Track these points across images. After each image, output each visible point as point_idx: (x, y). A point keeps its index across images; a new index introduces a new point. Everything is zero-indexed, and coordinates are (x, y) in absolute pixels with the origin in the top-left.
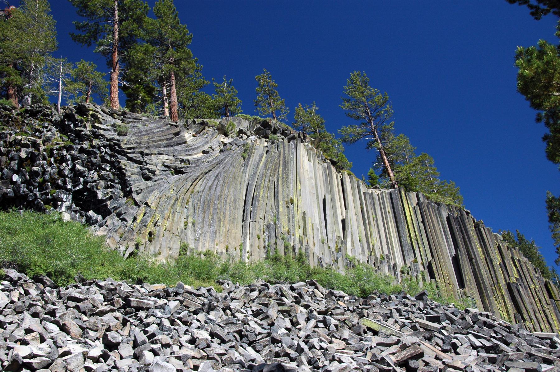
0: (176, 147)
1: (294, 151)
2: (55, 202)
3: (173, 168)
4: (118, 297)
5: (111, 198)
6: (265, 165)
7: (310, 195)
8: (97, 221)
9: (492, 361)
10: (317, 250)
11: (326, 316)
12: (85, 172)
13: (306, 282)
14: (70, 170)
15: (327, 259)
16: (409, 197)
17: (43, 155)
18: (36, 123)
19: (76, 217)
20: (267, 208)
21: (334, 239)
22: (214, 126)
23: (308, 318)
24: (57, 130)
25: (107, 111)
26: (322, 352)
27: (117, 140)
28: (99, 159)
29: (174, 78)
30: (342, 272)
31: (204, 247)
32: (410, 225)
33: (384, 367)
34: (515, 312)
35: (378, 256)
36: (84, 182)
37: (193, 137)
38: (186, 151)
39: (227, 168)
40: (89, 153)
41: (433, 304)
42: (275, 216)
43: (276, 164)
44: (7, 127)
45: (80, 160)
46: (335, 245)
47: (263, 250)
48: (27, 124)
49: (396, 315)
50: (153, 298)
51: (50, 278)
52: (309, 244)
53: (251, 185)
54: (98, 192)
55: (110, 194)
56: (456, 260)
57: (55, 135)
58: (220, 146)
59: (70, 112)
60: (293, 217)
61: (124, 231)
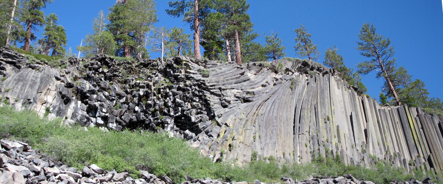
0: (243, 83)
1: (328, 82)
2: (163, 125)
3: (242, 99)
5: (201, 121)
6: (307, 93)
8: (192, 137)
10: (348, 153)
13: (344, 176)
14: (172, 102)
15: (357, 159)
16: (411, 111)
17: (154, 92)
18: (147, 71)
19: (177, 134)
20: (311, 124)
22: (268, 67)
24: (162, 75)
25: (194, 60)
27: (203, 81)
28: (191, 94)
29: (237, 34)
30: (368, 167)
32: (413, 131)
36: (181, 110)
39: (280, 97)
40: (184, 90)
42: (317, 130)
43: (315, 92)
44: (130, 75)
45: (179, 95)
46: (361, 148)
48: (142, 72)
51: (169, 177)
54: (192, 117)
55: (200, 118)
57: (161, 79)
58: (273, 81)
59: (170, 62)
60: (330, 130)
61: (212, 144)
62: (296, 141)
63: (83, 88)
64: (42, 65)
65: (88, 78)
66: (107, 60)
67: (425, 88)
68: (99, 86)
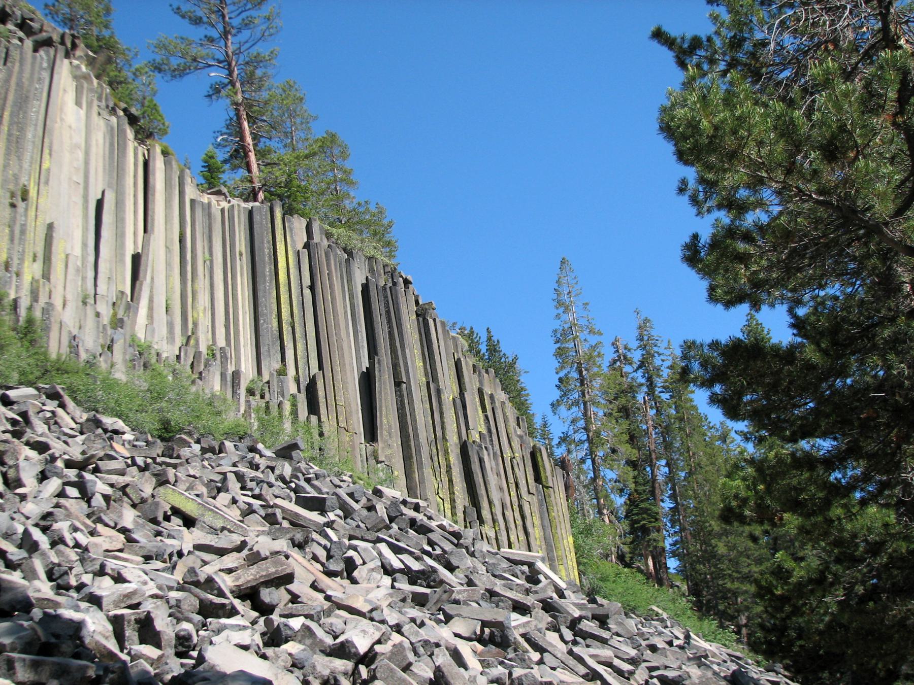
1: (46, 75)
9: (420, 601)
11: (84, 473)
13: (38, 389)
15: (90, 342)
21: (110, 297)
23: (42, 472)
26: (76, 552)
30: (120, 375)
33: (211, 597)
34: (467, 504)
35: (203, 349)
41: (311, 471)
46: (112, 311)
49: (234, 485)
52: (52, 301)
56: (368, 381)
60: (23, 232)
67: (348, 165)
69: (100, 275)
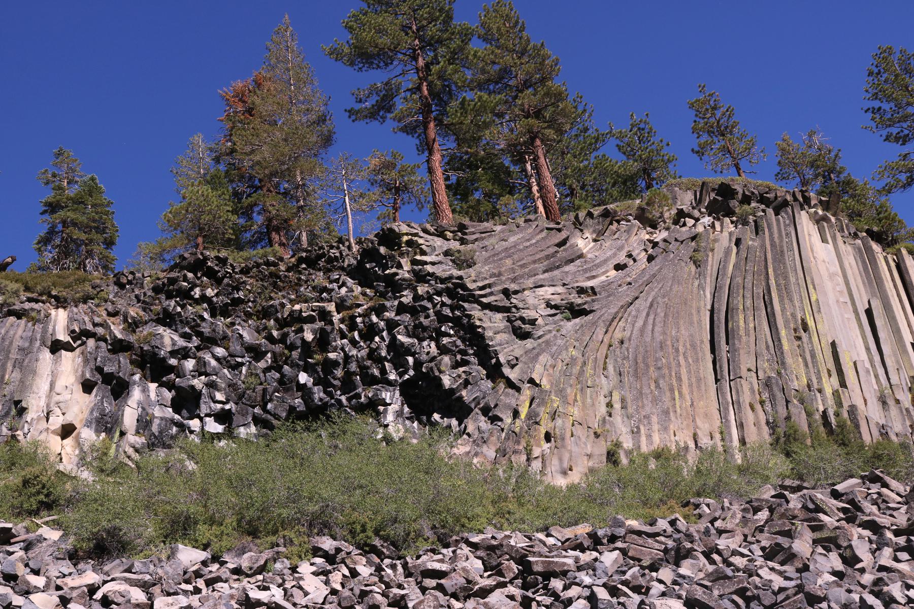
0: (567, 268)
2: (374, 407)
3: (566, 308)
4: (508, 560)
5: (466, 383)
7: (839, 307)
12: (413, 346)
17: (341, 330)
18: (319, 278)
19: (414, 428)
21: (904, 384)
28: (433, 317)
31: (652, 443)
37: (592, 244)
38: (585, 271)
40: (413, 310)
47: (766, 430)
48: (306, 282)
50: (571, 553)
53: (719, 311)
54: (442, 377)
55: (464, 376)
58: (646, 250)
59: (370, 245)
60: (813, 356)
62: (725, 398)
63: (157, 347)
64: (43, 302)
65: (167, 319)
66: (209, 264)
68: (199, 334)
69: (889, 369)
